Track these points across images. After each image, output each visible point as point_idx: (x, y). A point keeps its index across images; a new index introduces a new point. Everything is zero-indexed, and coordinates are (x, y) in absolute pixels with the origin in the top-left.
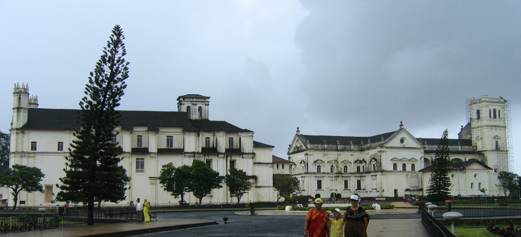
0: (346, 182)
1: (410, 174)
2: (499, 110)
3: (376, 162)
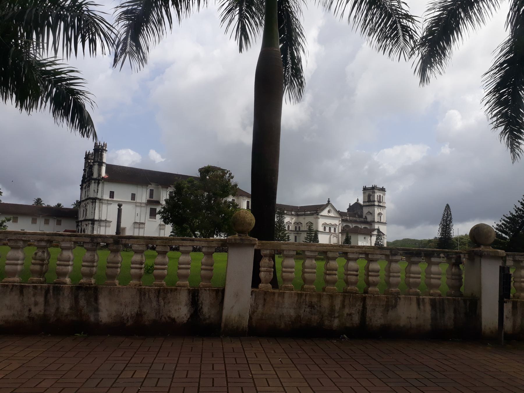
1: (333, 234)
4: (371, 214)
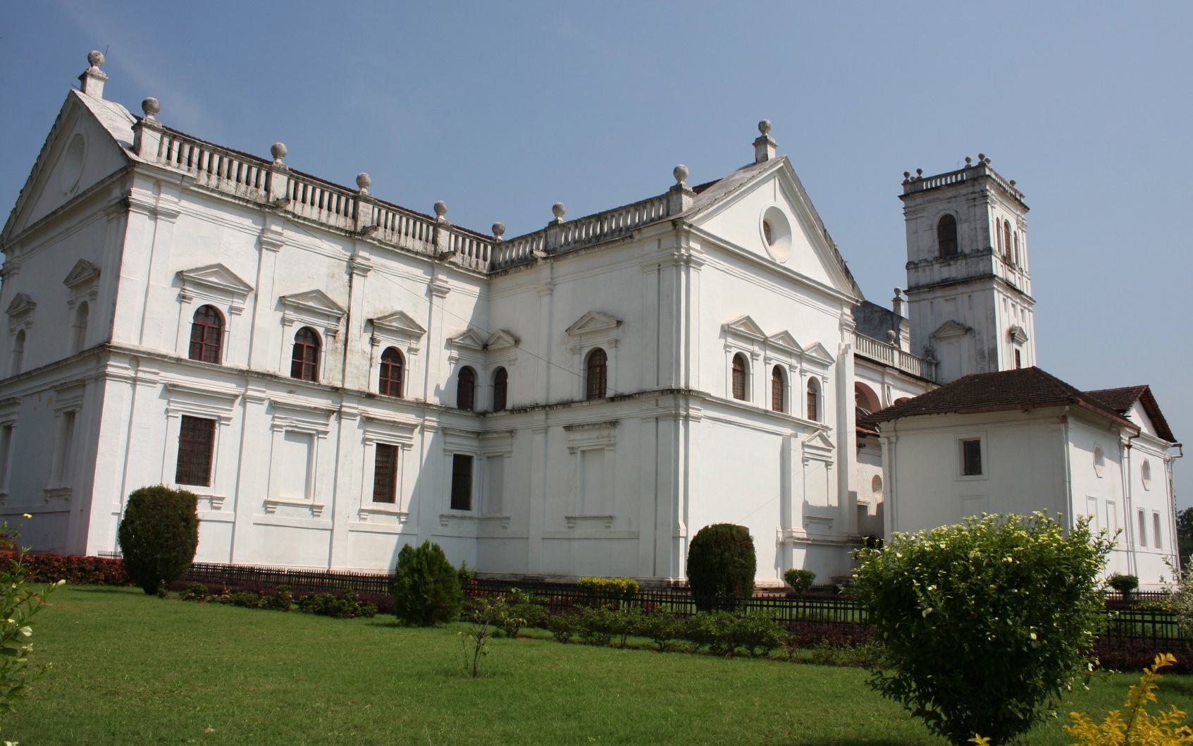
0: (387, 458)
2: (1015, 233)
3: (614, 334)
4: (968, 330)
